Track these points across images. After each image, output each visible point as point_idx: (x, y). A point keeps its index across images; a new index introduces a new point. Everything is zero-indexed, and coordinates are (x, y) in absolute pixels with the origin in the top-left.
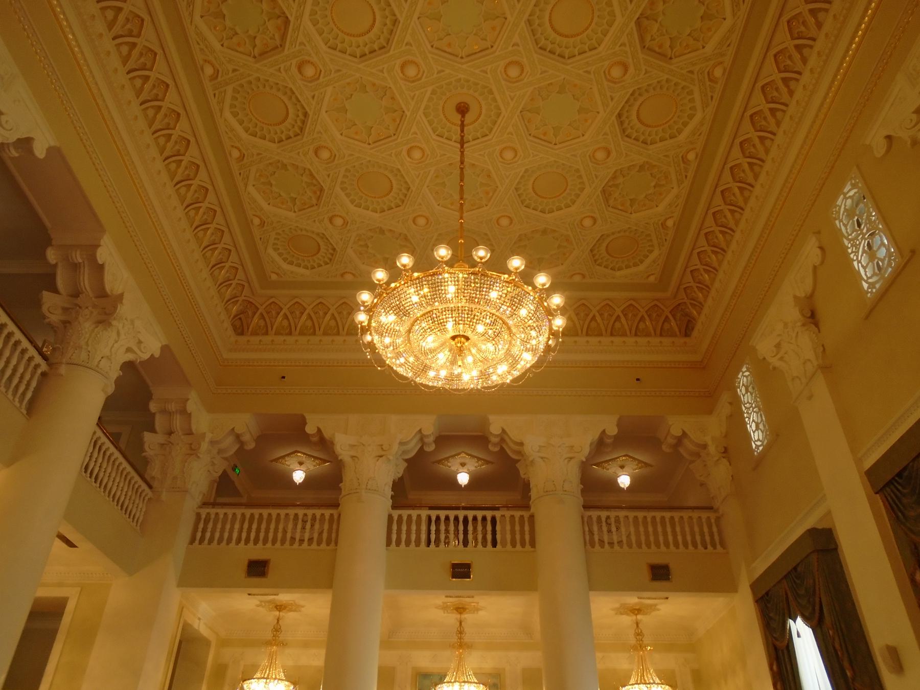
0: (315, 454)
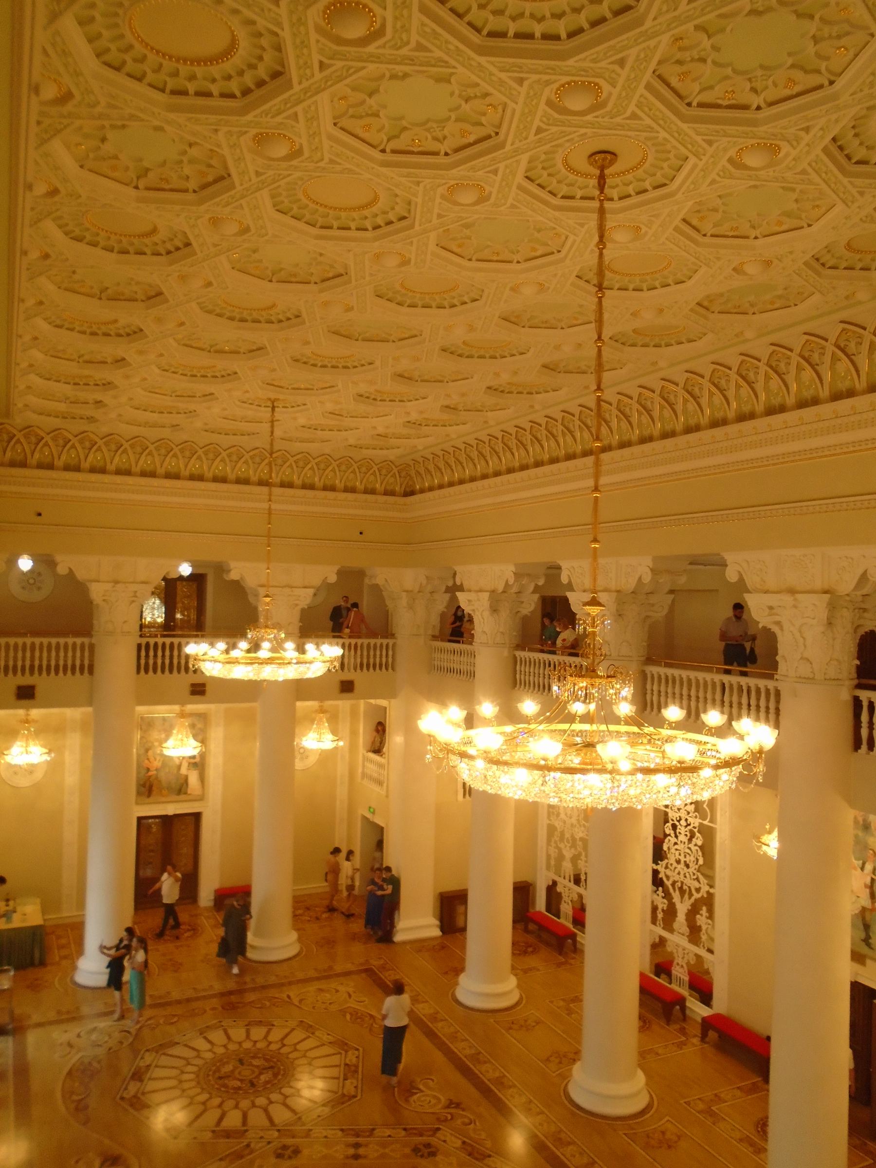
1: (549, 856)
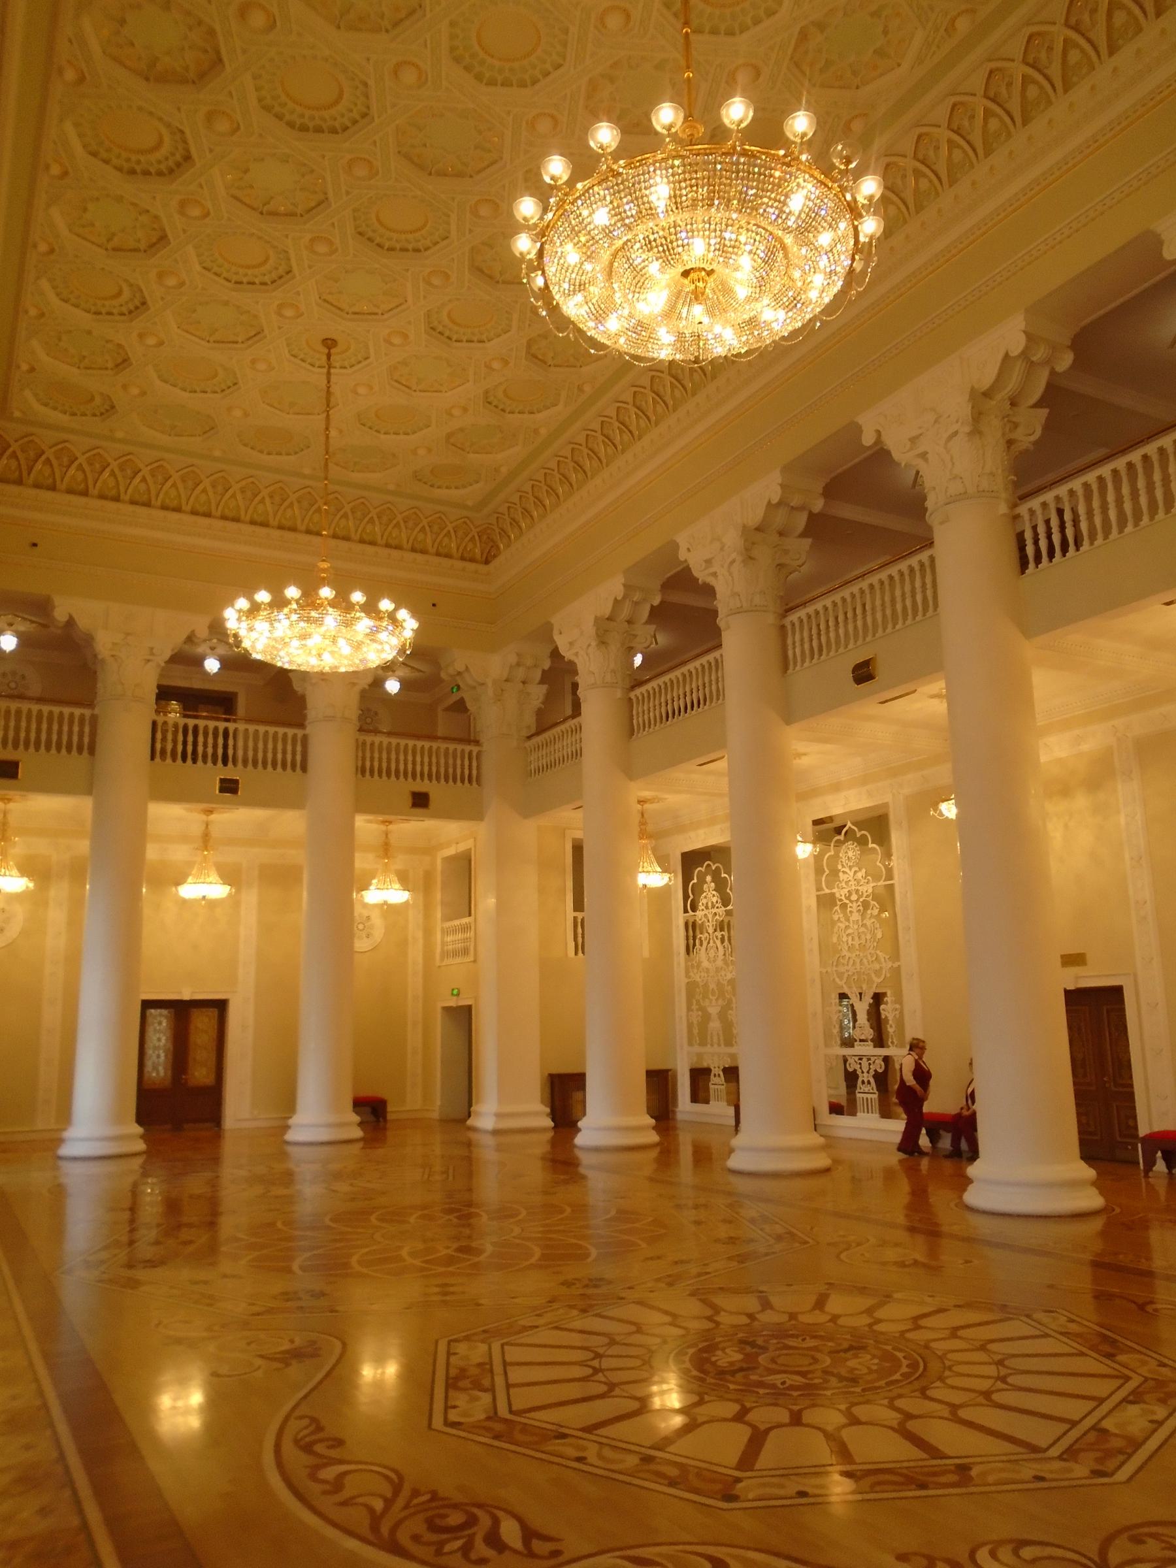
0: (33, 619)
1: (690, 1026)
